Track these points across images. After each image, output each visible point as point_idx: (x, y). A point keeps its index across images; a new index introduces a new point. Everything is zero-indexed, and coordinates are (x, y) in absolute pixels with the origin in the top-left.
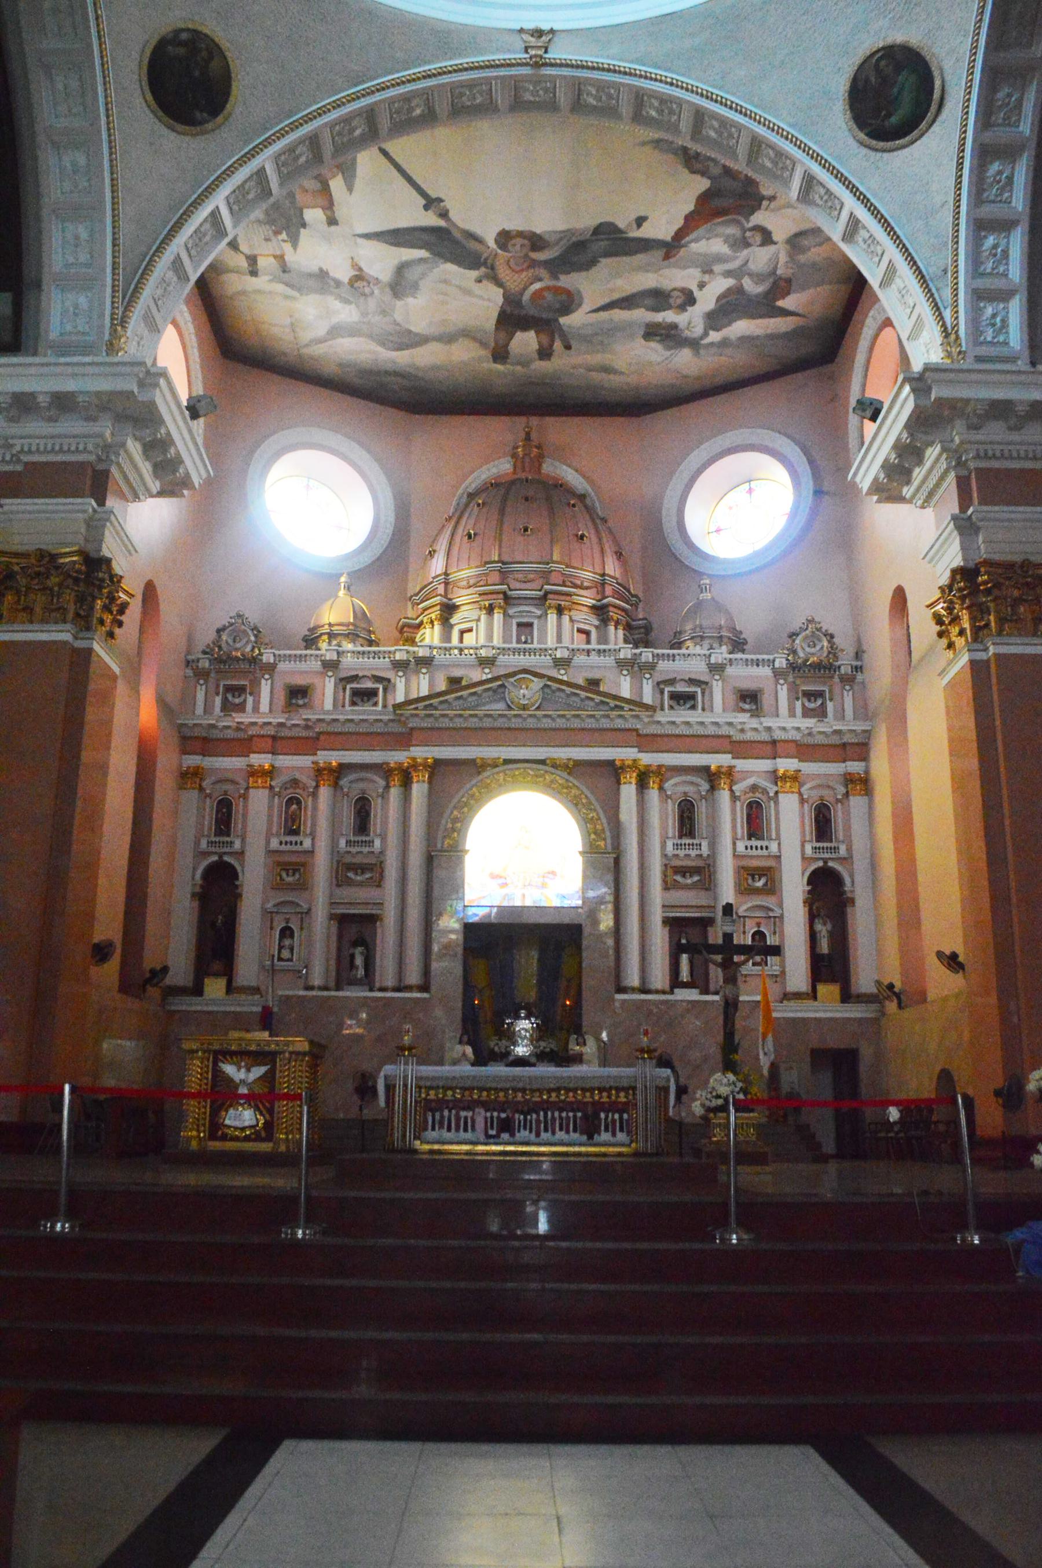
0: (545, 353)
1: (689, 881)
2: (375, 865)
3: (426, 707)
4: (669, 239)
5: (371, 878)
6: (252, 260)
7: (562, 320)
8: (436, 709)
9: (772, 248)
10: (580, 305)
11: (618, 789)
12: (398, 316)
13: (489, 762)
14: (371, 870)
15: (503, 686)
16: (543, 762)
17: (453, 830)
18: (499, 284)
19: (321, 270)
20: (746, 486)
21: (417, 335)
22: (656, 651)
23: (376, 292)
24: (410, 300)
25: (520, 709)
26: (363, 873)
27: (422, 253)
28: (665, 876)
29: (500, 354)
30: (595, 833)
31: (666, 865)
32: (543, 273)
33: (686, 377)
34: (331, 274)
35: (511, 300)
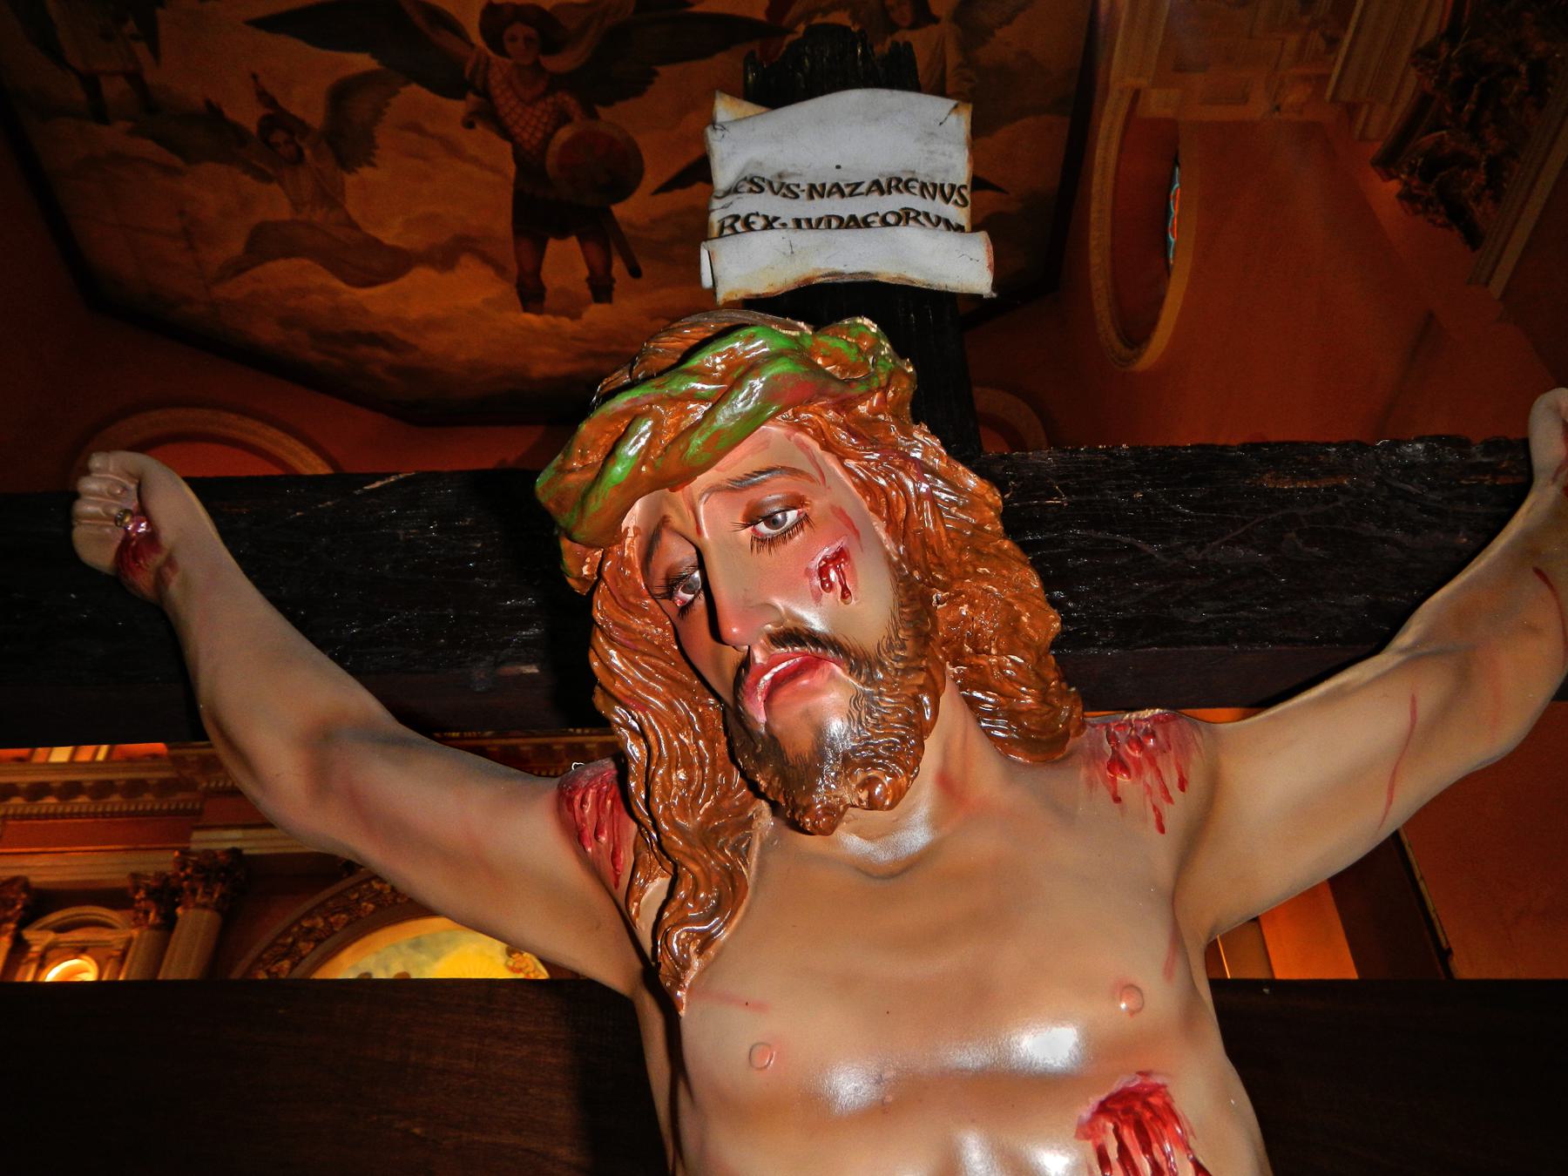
0: (601, 289)
4: (761, 16)
6: (91, 82)
7: (619, 210)
9: (934, 29)
10: (639, 175)
12: (353, 208)
18: (505, 133)
19: (209, 103)
21: (395, 251)
23: (307, 152)
24: (366, 172)
27: (362, 62)
29: (531, 295)
32: (570, 101)
34: (229, 113)
35: (529, 166)
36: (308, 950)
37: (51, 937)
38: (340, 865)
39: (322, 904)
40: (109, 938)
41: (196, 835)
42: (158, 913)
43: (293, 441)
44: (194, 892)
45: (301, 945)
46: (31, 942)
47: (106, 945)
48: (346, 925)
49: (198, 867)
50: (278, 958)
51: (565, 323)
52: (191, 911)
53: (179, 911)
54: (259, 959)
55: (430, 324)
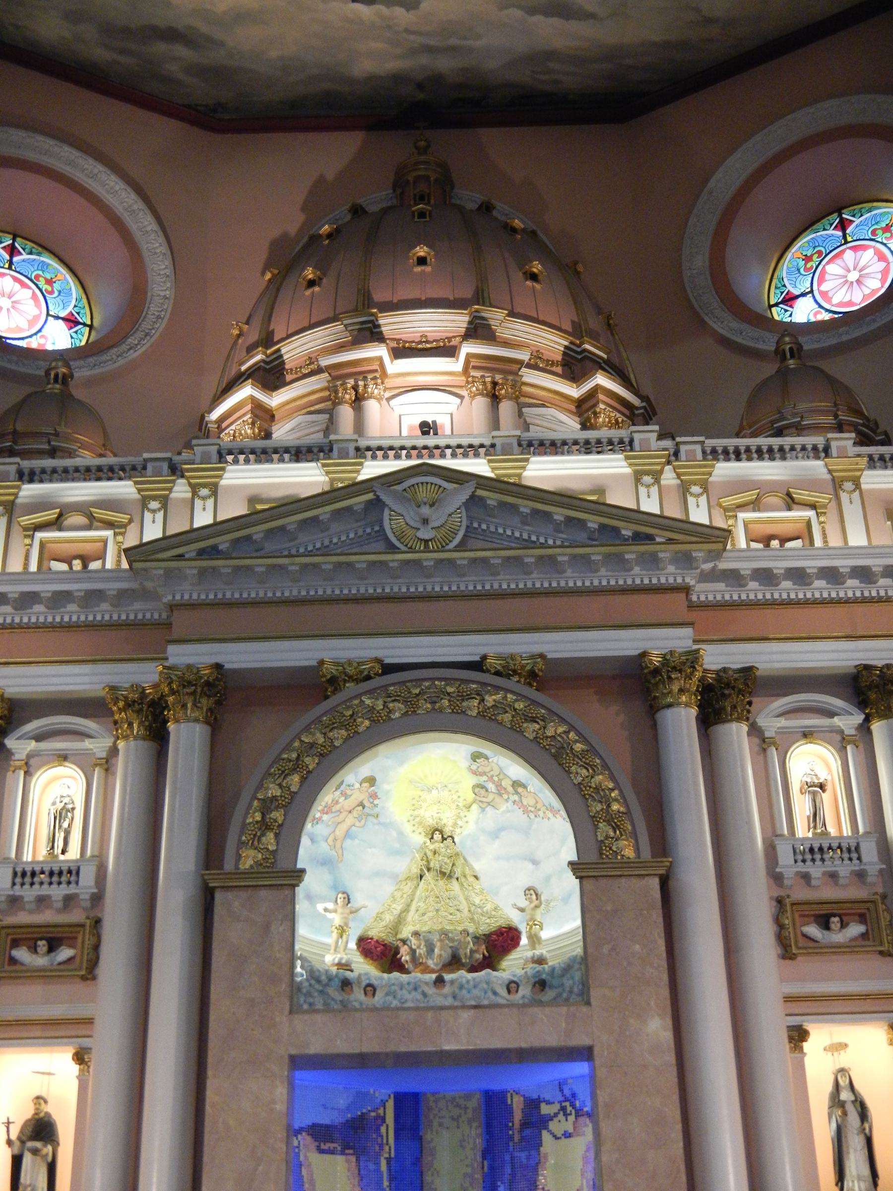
1: (838, 937)
2: (83, 926)
3: (202, 553)
5: (70, 960)
8: (226, 556)
11: (654, 726)
13: (351, 671)
14: (71, 941)
15: (377, 504)
16: (478, 666)
17: (265, 826)
20: (835, 219)
22: (710, 443)
25: (411, 550)
26: (53, 946)
28: (781, 926)
30: (608, 822)
31: (780, 901)
33: (708, 21)
36: (315, 765)
37: (33, 744)
38: (324, 679)
39: (318, 720)
40: (91, 746)
41: (172, 649)
42: (141, 723)
43: (91, 161)
44: (184, 706)
45: (307, 760)
46: (13, 751)
47: (87, 753)
48: (346, 740)
49: (185, 683)
50: (285, 774)
51: (399, 12)
52: (182, 725)
53: (171, 726)
54: (268, 774)
55: (240, 17)
